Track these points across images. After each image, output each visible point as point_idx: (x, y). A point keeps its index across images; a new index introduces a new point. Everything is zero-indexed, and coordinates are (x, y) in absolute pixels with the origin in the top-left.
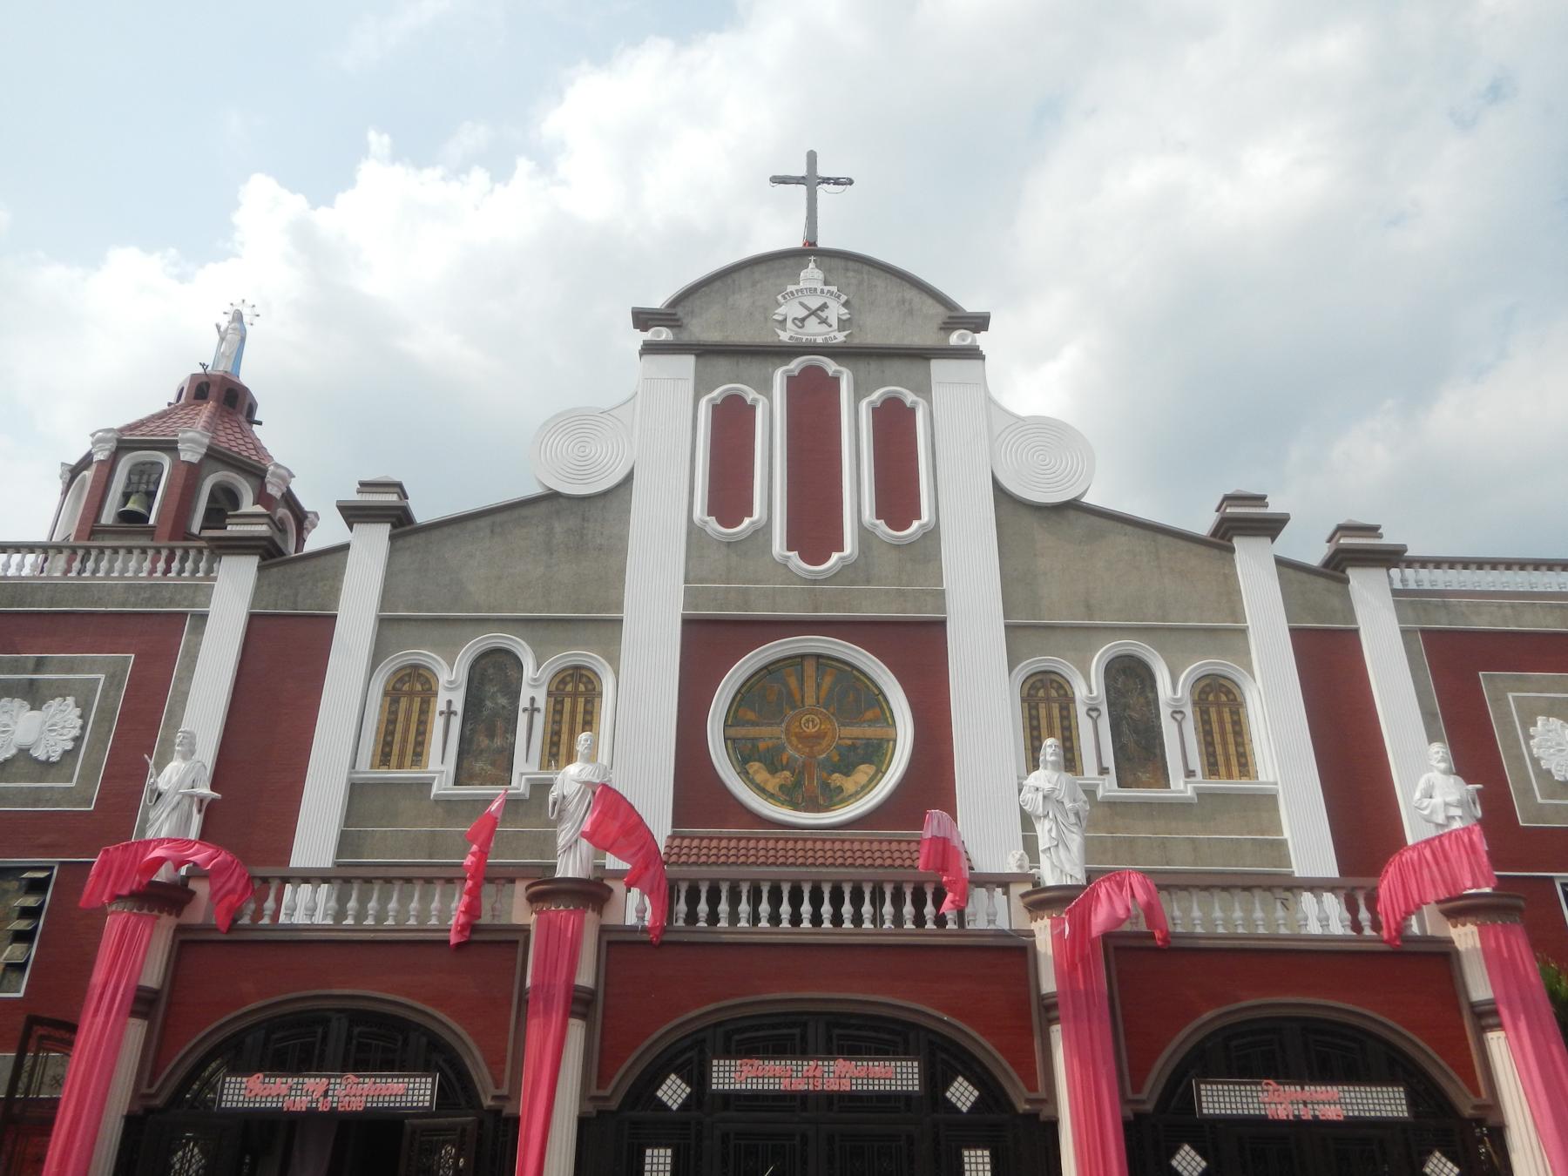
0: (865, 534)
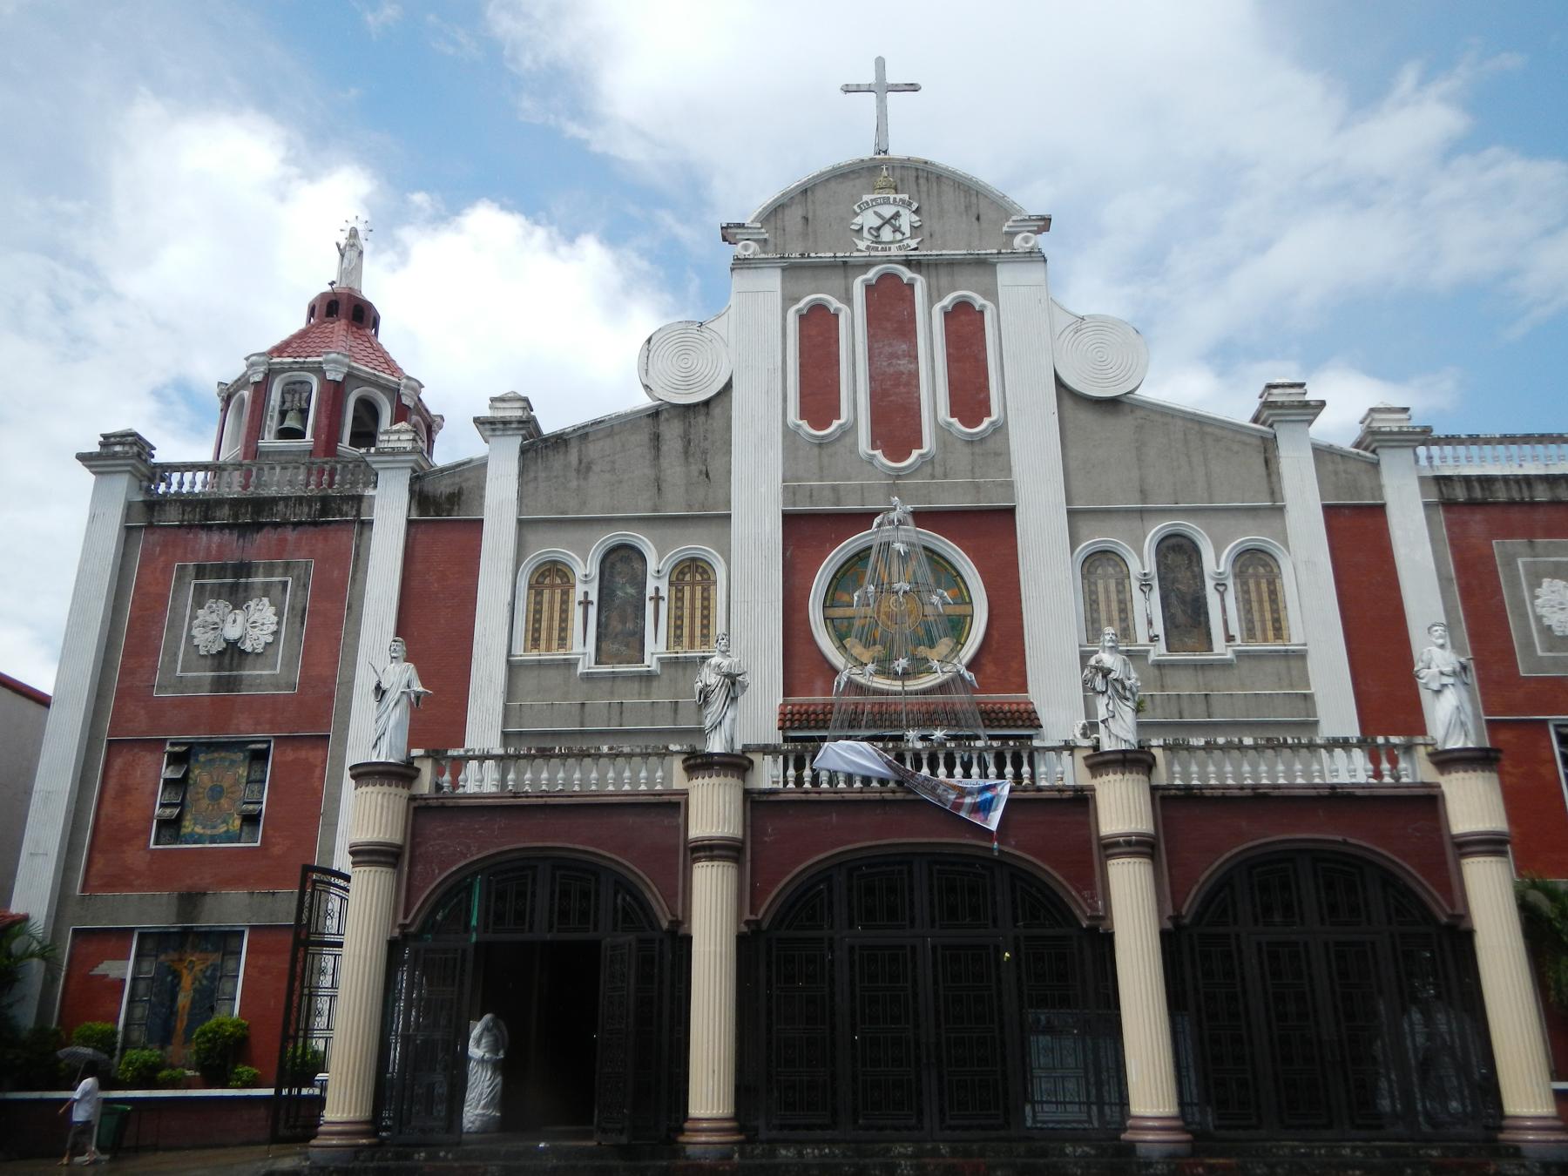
0: (942, 431)
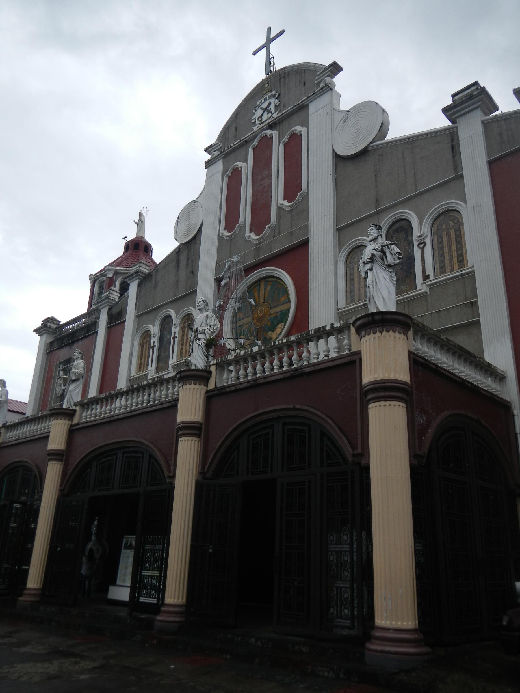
0: (280, 209)
